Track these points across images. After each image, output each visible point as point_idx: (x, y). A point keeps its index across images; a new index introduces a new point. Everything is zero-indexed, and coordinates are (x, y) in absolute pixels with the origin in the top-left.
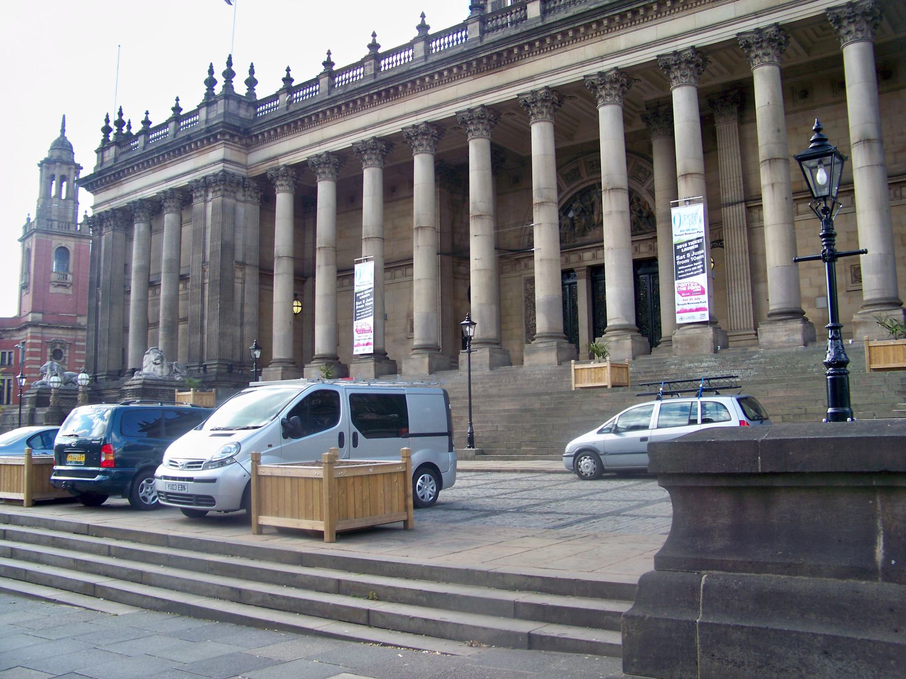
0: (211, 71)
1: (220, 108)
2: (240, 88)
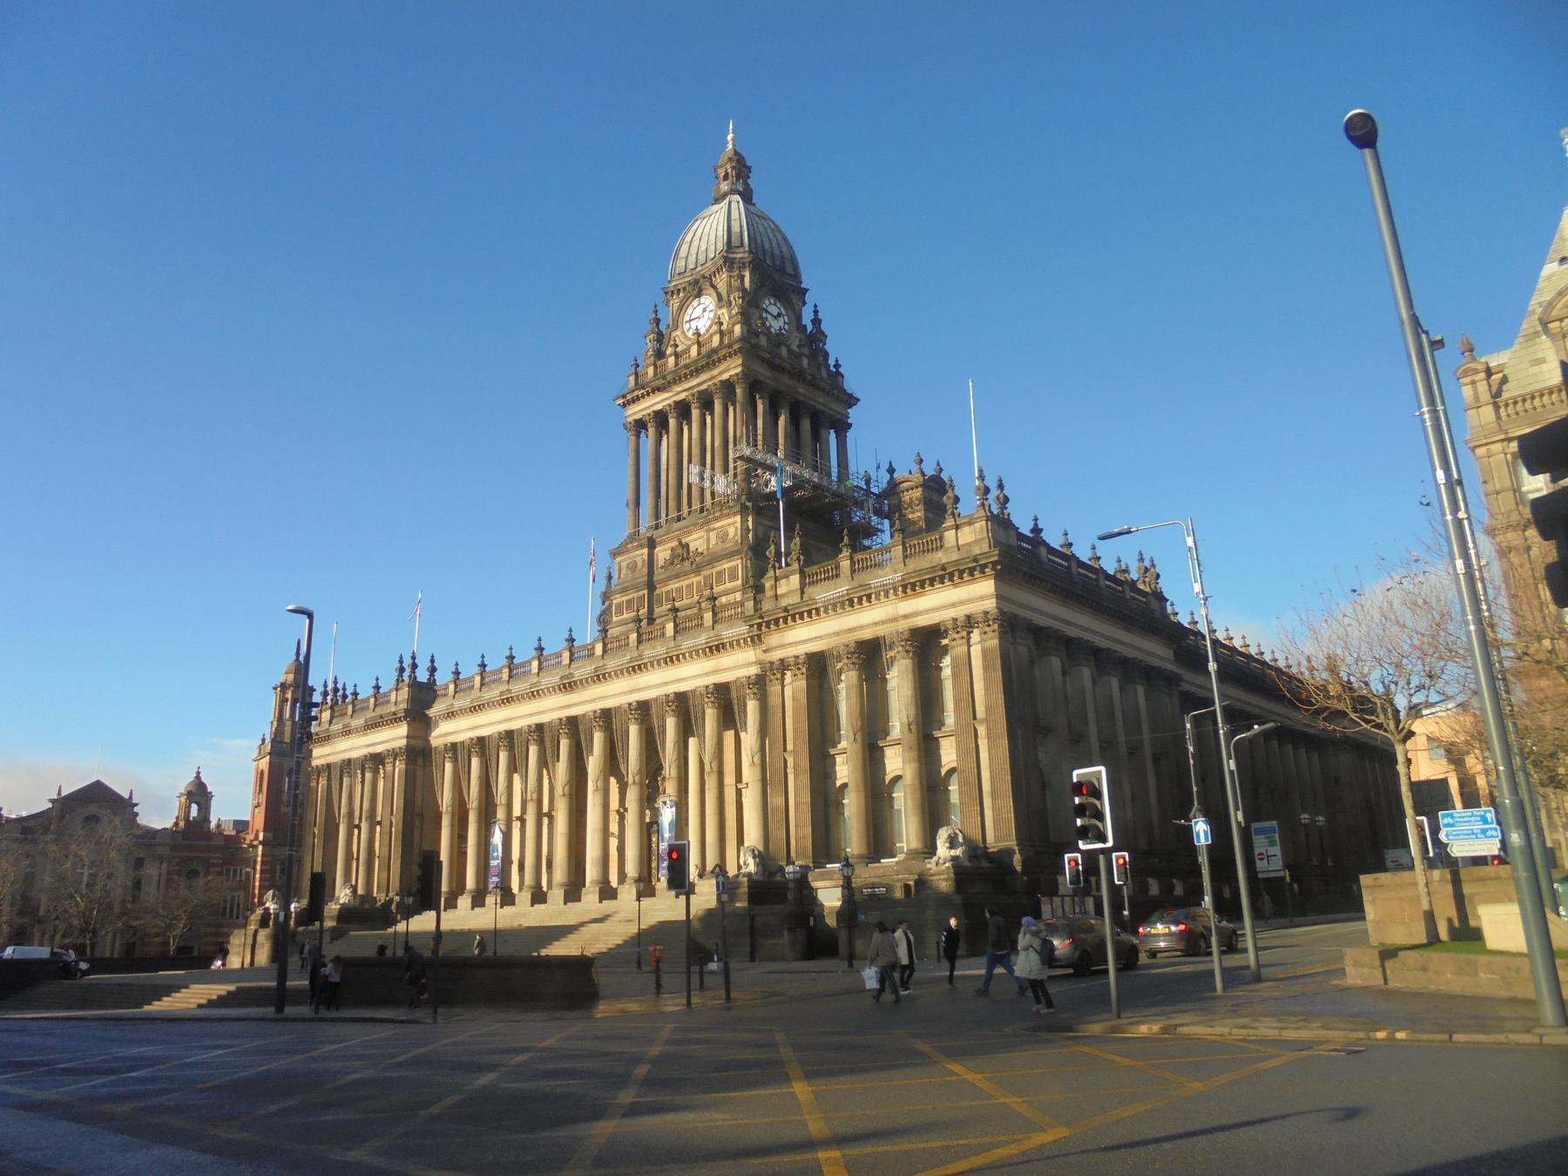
0: (401, 662)
1: (404, 693)
2: (422, 676)
